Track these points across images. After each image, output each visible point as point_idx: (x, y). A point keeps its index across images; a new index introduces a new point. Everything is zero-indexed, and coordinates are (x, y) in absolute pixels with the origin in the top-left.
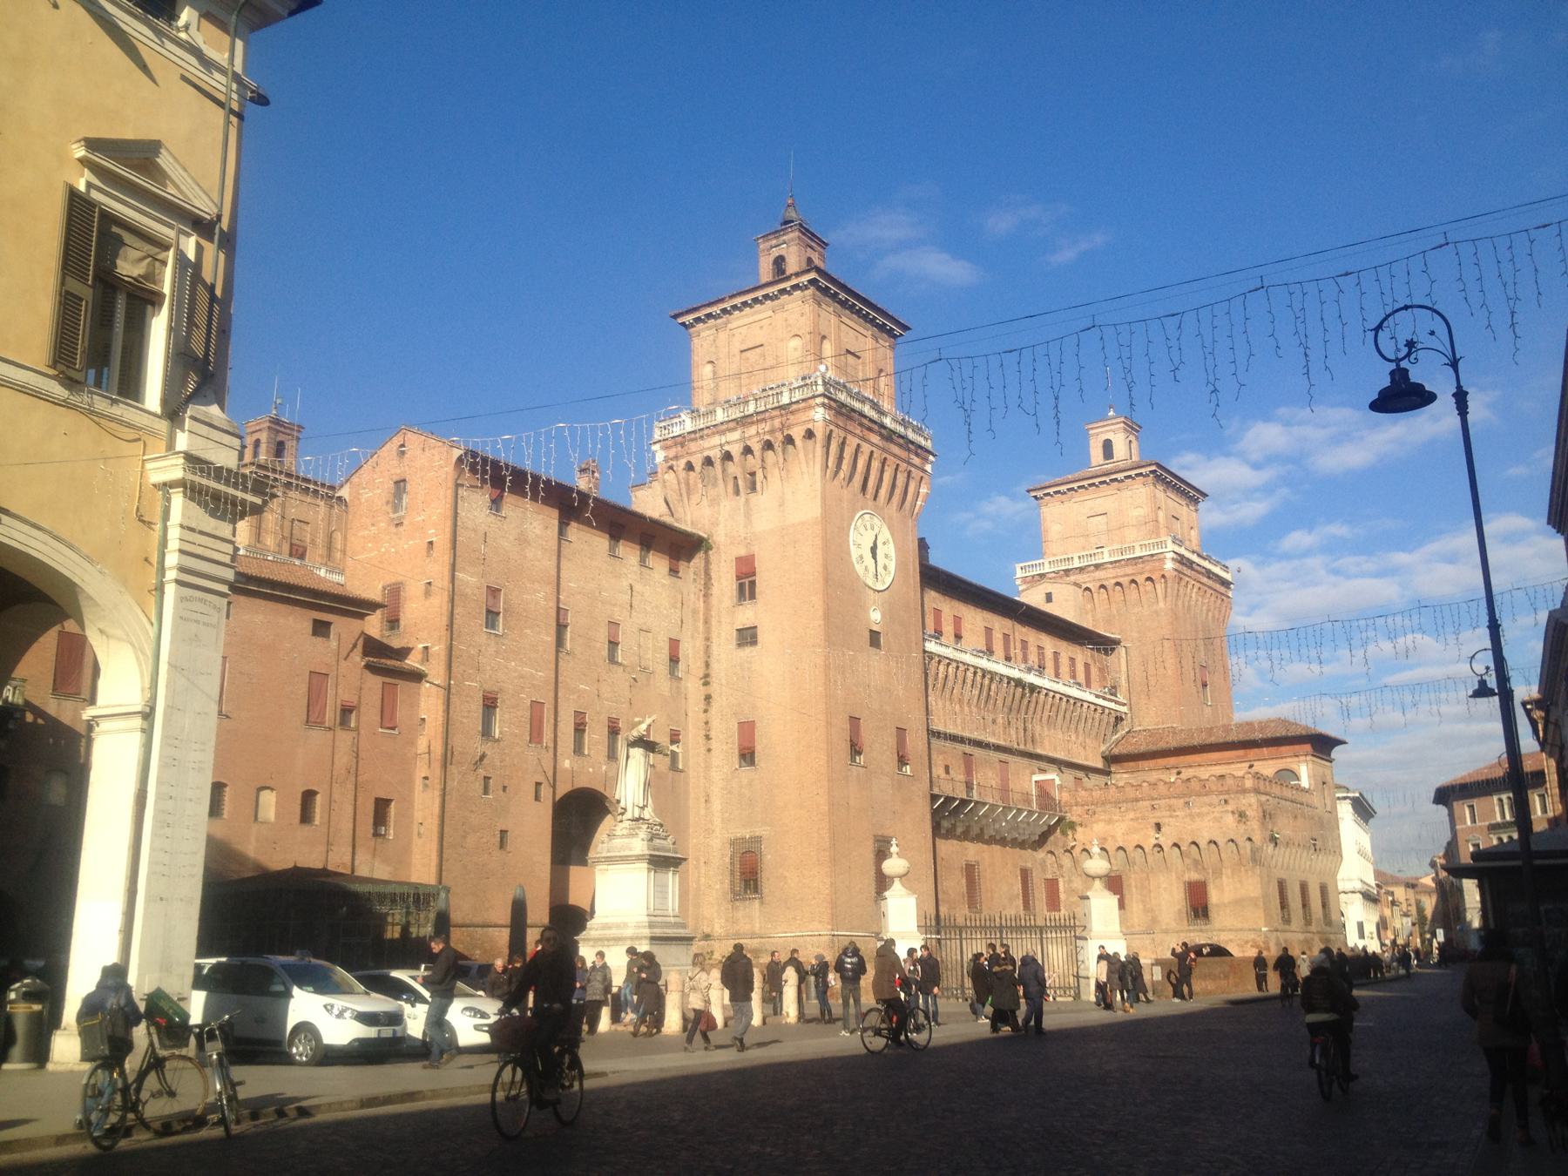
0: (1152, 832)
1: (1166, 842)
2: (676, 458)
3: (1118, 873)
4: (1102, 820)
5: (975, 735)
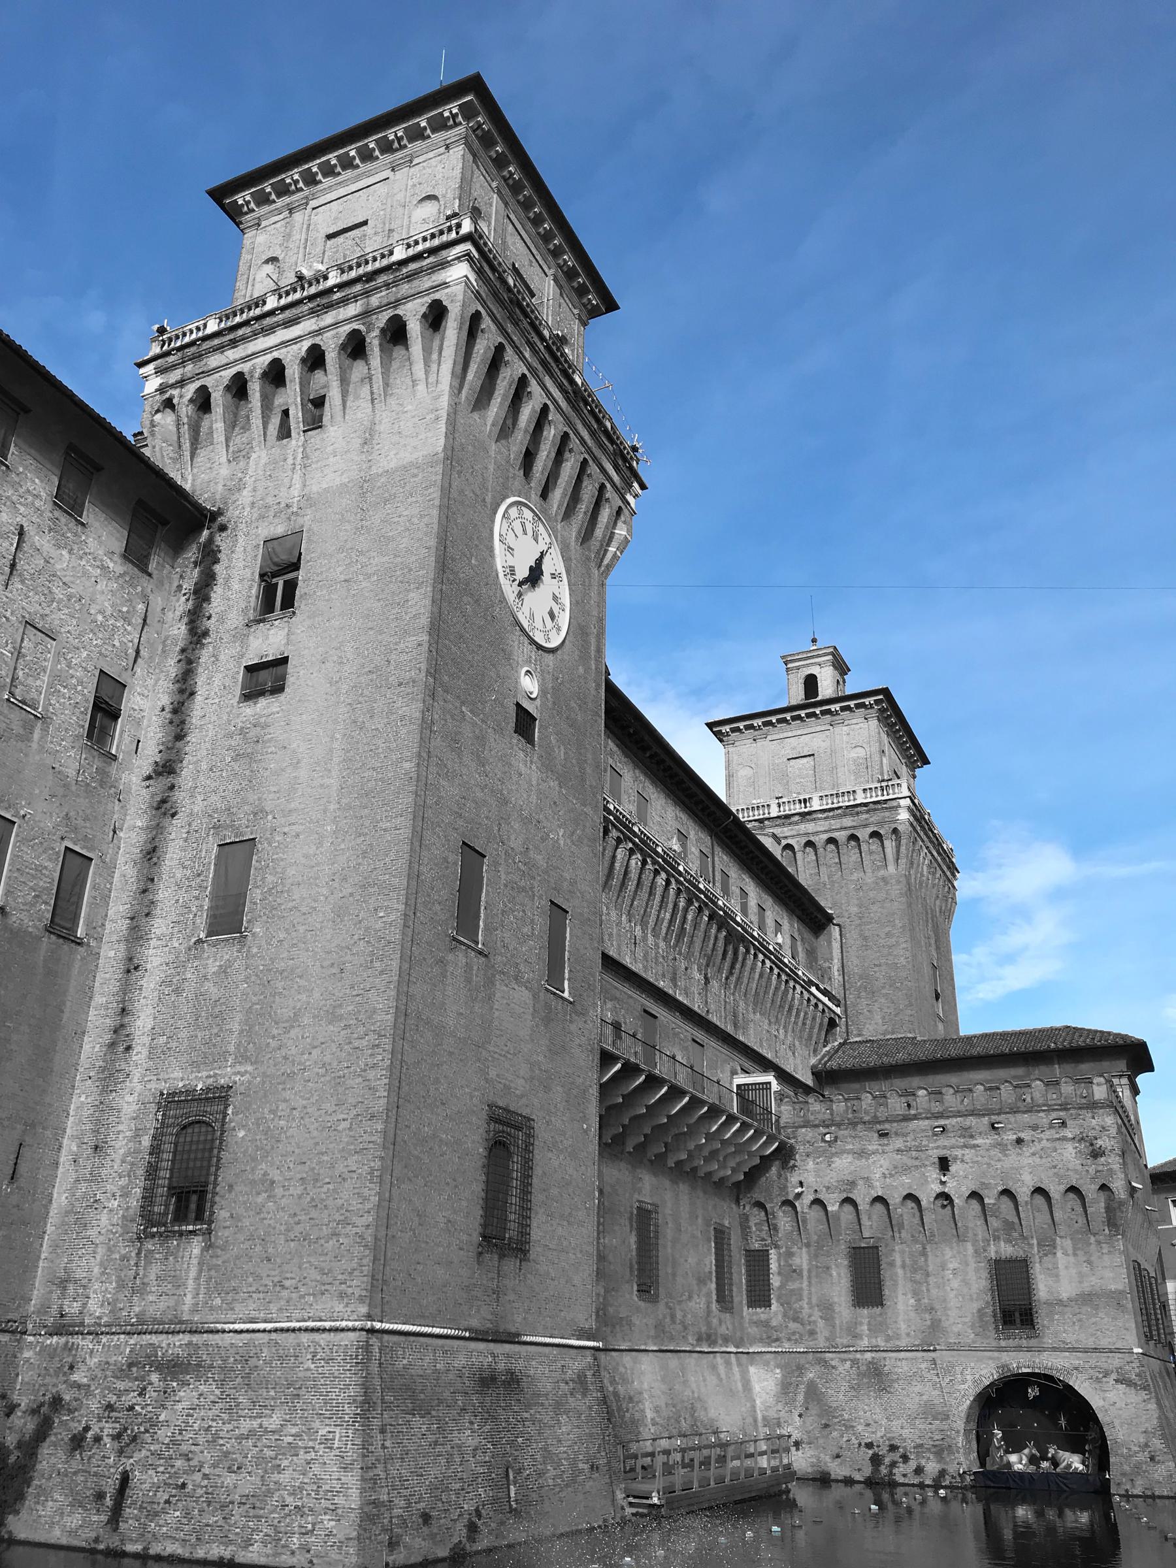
0: (933, 1173)
2: (181, 383)
4: (849, 1152)
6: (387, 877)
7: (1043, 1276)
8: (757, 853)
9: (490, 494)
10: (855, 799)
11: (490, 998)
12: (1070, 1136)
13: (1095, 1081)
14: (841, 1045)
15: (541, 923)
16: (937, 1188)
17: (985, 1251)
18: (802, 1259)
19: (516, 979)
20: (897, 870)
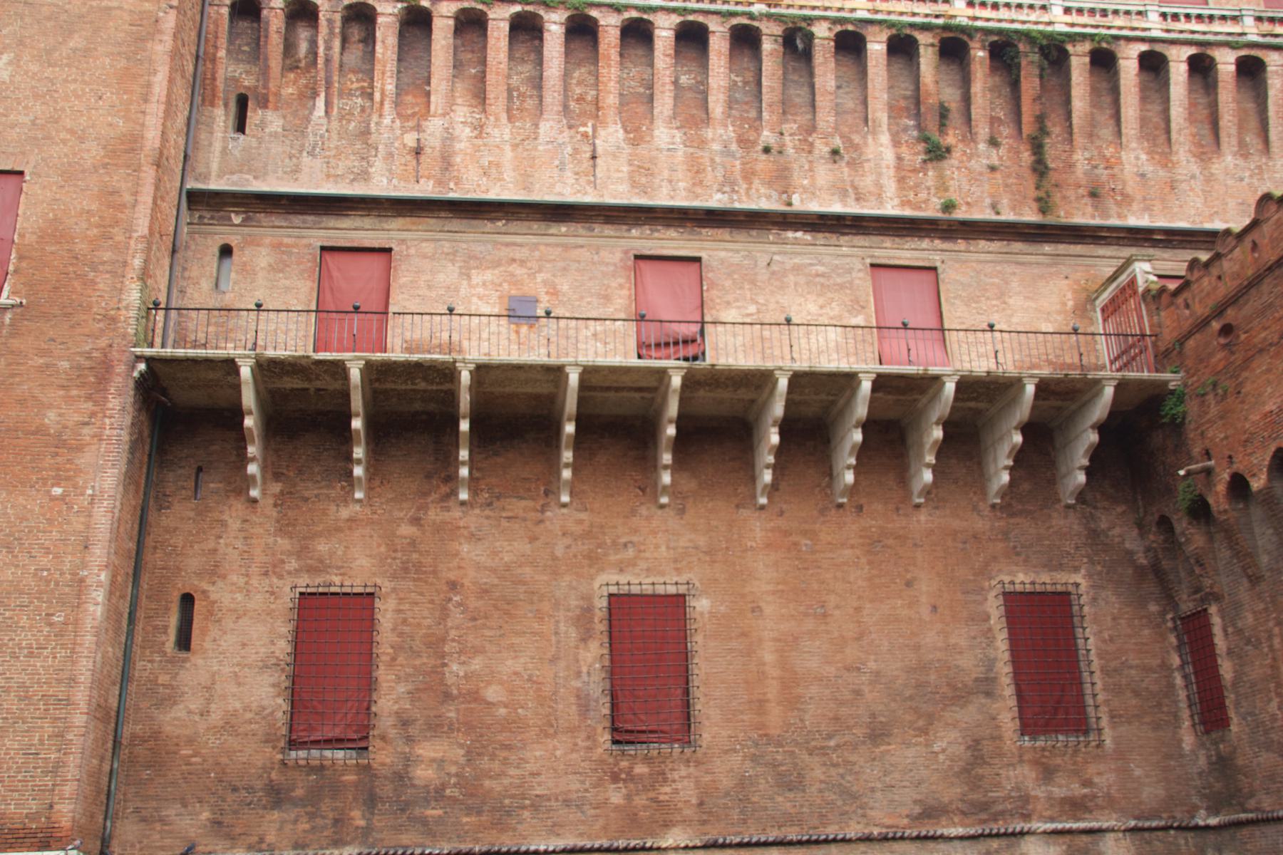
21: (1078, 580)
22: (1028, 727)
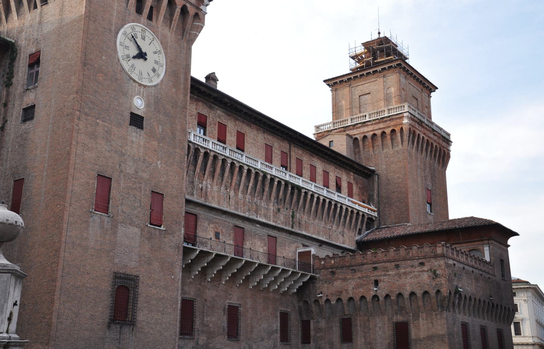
1: (381, 294)
3: (349, 316)
4: (340, 279)
5: (247, 215)
6: (61, 192)
7: (414, 329)
8: (319, 148)
9: (114, 26)
10: (384, 115)
11: (115, 233)
12: (426, 269)
13: (438, 246)
14: (377, 229)
15: (146, 201)
16: (373, 293)
17: (392, 319)
18: (323, 324)
19: (130, 224)
20: (402, 146)
21: (289, 310)
22: (281, 341)
